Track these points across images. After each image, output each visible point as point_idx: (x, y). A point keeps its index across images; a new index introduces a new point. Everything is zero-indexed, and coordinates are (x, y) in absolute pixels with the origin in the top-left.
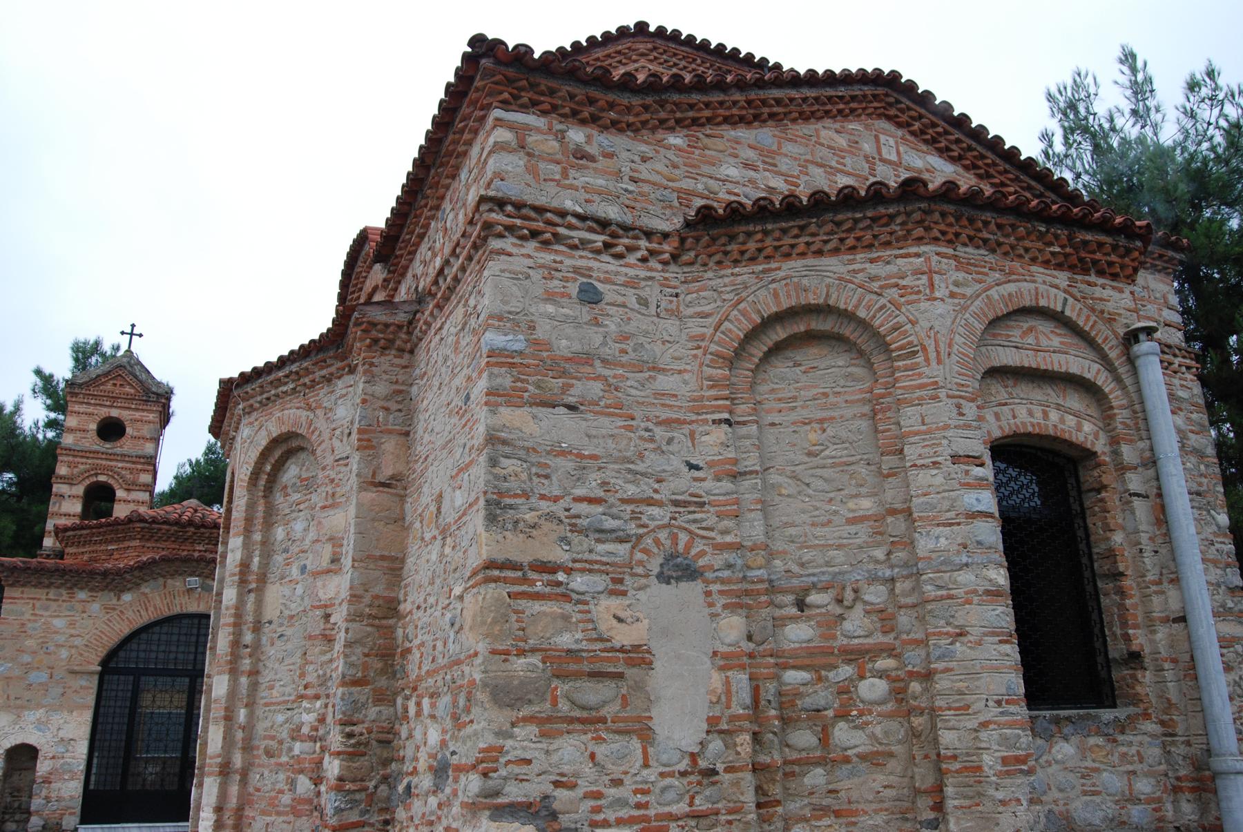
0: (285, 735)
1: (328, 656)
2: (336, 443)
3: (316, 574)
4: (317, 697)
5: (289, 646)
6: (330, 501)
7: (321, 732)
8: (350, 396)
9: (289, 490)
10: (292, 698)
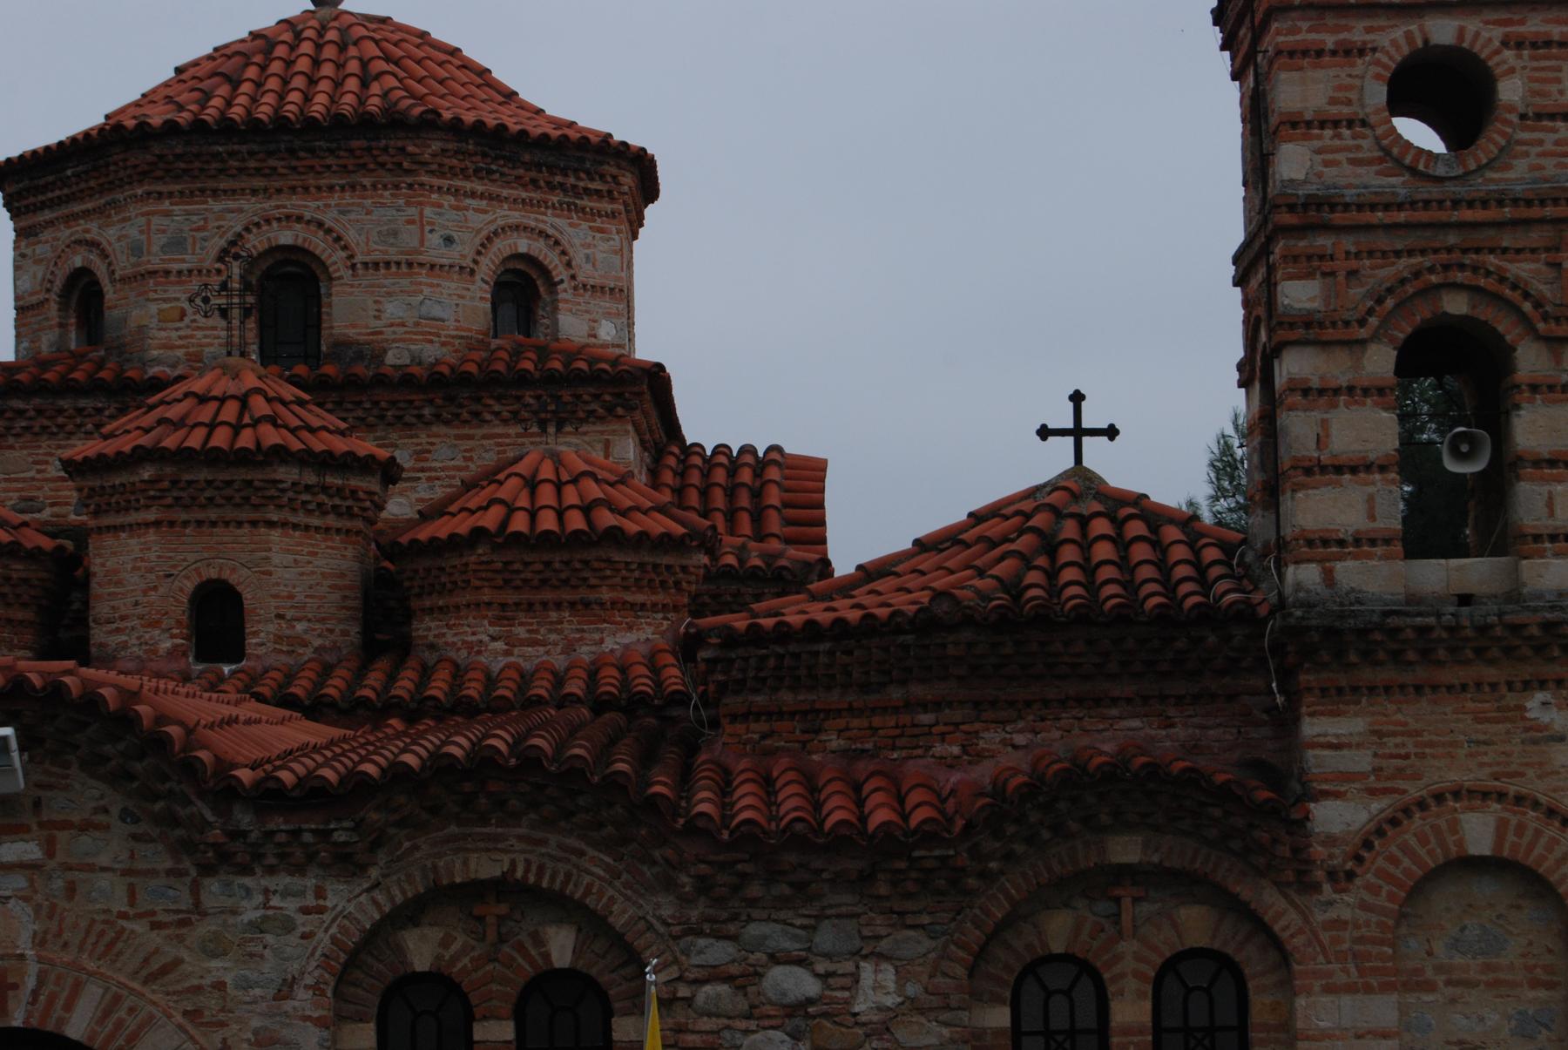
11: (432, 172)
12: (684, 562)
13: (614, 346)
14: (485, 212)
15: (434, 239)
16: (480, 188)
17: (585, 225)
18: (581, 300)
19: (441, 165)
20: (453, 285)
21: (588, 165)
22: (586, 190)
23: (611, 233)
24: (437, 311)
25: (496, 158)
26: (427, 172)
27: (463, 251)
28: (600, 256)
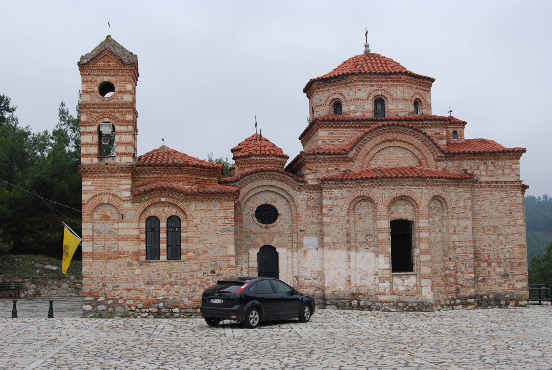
0: (440, 269)
1: (454, 253)
2: (452, 203)
3: (451, 234)
4: (453, 261)
5: (438, 249)
7: (455, 269)
15: (318, 101)
16: (326, 89)
17: (347, 89)
24: (318, 113)
27: (323, 101)
28: (351, 94)
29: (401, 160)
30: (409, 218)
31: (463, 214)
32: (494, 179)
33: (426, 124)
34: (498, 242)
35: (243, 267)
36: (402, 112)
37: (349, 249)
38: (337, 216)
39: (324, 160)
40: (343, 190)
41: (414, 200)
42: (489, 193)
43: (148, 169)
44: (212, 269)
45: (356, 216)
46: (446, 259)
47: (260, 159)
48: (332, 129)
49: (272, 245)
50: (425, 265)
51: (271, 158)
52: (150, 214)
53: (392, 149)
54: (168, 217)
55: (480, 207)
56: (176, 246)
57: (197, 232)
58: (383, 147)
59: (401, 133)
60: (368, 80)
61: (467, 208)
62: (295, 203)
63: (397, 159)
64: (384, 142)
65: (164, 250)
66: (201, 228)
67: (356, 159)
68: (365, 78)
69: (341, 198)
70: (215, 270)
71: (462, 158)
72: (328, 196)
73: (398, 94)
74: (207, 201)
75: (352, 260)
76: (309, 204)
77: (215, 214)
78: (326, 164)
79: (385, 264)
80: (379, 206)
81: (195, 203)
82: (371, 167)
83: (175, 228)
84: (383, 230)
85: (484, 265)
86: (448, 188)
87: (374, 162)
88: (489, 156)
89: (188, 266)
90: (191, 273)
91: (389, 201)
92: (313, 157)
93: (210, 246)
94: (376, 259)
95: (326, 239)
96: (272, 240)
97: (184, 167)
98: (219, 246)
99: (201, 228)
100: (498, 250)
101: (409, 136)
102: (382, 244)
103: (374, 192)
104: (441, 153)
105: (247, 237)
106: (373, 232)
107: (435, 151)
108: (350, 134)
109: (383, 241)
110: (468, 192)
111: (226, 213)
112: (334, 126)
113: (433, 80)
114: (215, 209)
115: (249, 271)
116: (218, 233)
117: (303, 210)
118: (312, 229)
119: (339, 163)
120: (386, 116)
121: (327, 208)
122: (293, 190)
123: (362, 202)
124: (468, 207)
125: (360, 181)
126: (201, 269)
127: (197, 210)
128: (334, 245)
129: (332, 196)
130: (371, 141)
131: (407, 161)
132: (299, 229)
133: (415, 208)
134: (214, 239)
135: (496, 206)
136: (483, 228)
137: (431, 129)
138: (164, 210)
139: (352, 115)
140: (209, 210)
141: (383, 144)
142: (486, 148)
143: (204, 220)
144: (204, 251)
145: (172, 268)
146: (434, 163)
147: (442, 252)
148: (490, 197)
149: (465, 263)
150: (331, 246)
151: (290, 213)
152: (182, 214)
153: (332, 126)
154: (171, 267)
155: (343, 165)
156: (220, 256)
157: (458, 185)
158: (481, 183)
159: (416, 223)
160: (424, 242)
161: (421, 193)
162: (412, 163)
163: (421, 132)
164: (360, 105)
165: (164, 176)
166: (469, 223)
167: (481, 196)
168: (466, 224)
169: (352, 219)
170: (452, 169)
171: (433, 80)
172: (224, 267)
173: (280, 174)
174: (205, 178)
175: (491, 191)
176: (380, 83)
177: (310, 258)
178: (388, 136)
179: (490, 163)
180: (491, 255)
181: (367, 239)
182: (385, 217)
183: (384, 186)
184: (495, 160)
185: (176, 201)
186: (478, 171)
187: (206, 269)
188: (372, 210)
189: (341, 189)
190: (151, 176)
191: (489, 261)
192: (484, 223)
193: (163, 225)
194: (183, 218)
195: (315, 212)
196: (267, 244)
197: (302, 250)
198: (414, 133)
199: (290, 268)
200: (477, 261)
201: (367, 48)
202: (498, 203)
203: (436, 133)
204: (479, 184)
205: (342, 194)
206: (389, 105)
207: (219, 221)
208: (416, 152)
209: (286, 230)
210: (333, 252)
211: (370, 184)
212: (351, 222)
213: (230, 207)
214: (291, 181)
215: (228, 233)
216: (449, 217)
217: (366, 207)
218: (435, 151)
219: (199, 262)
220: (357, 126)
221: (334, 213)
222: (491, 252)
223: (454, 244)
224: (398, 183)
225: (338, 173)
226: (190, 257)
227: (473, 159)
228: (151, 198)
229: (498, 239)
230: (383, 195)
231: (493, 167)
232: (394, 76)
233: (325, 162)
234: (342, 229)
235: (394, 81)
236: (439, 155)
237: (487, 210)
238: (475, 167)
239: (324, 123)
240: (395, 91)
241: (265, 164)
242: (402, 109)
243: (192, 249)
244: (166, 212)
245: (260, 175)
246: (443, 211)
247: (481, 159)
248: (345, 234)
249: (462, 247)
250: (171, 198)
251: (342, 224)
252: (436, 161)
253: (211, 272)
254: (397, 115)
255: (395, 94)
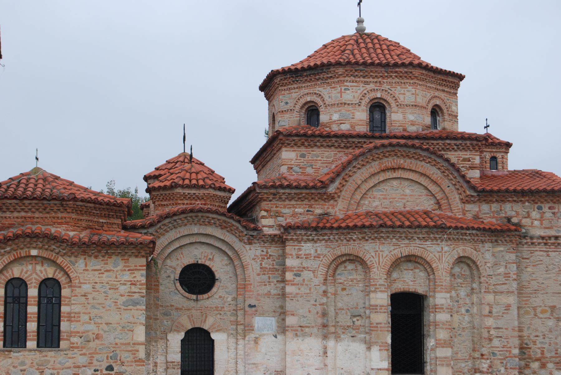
0: (466, 371)
1: (489, 346)
2: (487, 269)
4: (488, 359)
6: (487, 290)
7: (490, 370)
8: (491, 251)
9: (456, 277)
10: (467, 358)
11: (281, 86)
12: (173, 192)
13: (337, 121)
14: (297, 92)
15: (283, 104)
16: (296, 86)
17: (329, 87)
18: (327, 110)
19: (283, 83)
20: (288, 115)
21: (325, 70)
22: (328, 77)
23: (337, 87)
24: (282, 123)
25: (297, 77)
26: (281, 86)
27: (290, 105)
28: (333, 95)
29: (410, 199)
30: (421, 290)
31: (503, 286)
32: (553, 233)
33: (449, 144)
34: (556, 331)
35: (158, 361)
36: (413, 125)
37: (325, 337)
38: (307, 285)
39: (290, 196)
40: (317, 245)
41: (428, 263)
42: (545, 254)
43: (11, 204)
44: (108, 364)
45: (337, 285)
46: (477, 355)
47: (190, 192)
48: (303, 149)
49: (204, 328)
50: (443, 365)
51: (206, 192)
52: (13, 274)
53: (395, 183)
54: (41, 280)
55: (530, 275)
56: (53, 326)
57: (86, 304)
58: (382, 179)
59: (410, 158)
60: (362, 74)
61: (509, 277)
62: (242, 263)
63: (403, 199)
64: (383, 171)
65: (33, 332)
66: (94, 299)
67: (339, 197)
68: (356, 71)
69: (315, 257)
70: (114, 365)
71: (503, 199)
72: (294, 253)
73: (407, 98)
74: (103, 256)
75: (328, 354)
76: (263, 265)
77: (116, 278)
78: (293, 202)
79: (382, 361)
80: (374, 270)
81: (85, 259)
82: (363, 210)
83: (52, 298)
84: (378, 308)
85: (535, 365)
86: (481, 245)
87: (367, 202)
88: (546, 196)
89: (70, 358)
90: (75, 369)
91: (389, 263)
92: (272, 191)
93: (106, 328)
94: (368, 353)
95: (290, 321)
96: (205, 321)
97: (68, 203)
98: (120, 328)
99: (94, 299)
100: (556, 344)
101: (423, 163)
102: (377, 331)
103: (367, 248)
104: (472, 191)
105: (165, 314)
106: (362, 310)
107: (462, 187)
108: (331, 157)
109: (379, 326)
110: (512, 253)
111: (134, 275)
112: (306, 143)
113: (461, 77)
114: (115, 269)
115: (168, 368)
116: (120, 306)
117: (255, 275)
118: (269, 304)
119: (312, 202)
120: (388, 131)
121: (293, 271)
122: (239, 243)
123: (347, 263)
124: (511, 275)
125: (345, 231)
126: (92, 363)
127: (87, 270)
128: (302, 330)
129: (300, 253)
130: (364, 168)
131: (418, 201)
132: (247, 303)
133: (429, 276)
134: (114, 317)
135: (554, 275)
136: (535, 309)
137: (456, 153)
138: (34, 269)
139: (335, 128)
140: (107, 271)
141: (382, 174)
142: (541, 185)
143: (98, 286)
144: (98, 334)
145: (46, 360)
146: (460, 206)
147: (470, 345)
148: (546, 260)
149: (505, 362)
150: (297, 330)
151: (234, 278)
152: (63, 275)
153: (303, 144)
154: (43, 359)
155: (319, 204)
156: (122, 344)
157: (496, 241)
158: (532, 238)
159: (431, 299)
160: (443, 328)
161: (438, 252)
162: (427, 204)
163: (441, 157)
164: (348, 113)
165: (37, 215)
166: (512, 300)
167: (532, 259)
168: (509, 302)
169: (331, 290)
170: (488, 215)
171: (461, 77)
172: (128, 362)
173: (219, 217)
174: (101, 221)
175: (548, 251)
176: (380, 79)
177: (263, 350)
178: (389, 162)
179: (547, 208)
180: (545, 350)
181: (353, 322)
182: (383, 288)
183: (382, 239)
184: (554, 203)
185: (54, 255)
186: (528, 219)
187: (99, 363)
188: (362, 277)
189: (316, 242)
190: (16, 214)
191: (543, 360)
192: (536, 301)
193: (33, 292)
194: (64, 282)
195: (274, 277)
196: (197, 326)
197: (252, 336)
198: (430, 158)
199: (232, 365)
200: (525, 359)
201: (360, 25)
202: (558, 269)
203: (464, 160)
204: (529, 240)
205: (316, 251)
206: (392, 114)
207: (123, 289)
208: (433, 188)
209: (227, 304)
210: (300, 340)
211: (360, 236)
212: (329, 295)
213: (140, 266)
214: (237, 228)
215: (135, 308)
216: (483, 290)
217: (354, 272)
218: (462, 187)
219: (88, 353)
220: (342, 145)
221: (304, 280)
222: (546, 346)
223: (489, 332)
224: (403, 235)
225: (311, 217)
226: (73, 344)
227: (521, 201)
228: (15, 250)
229: (557, 326)
230: (381, 253)
231: (551, 215)
232: (401, 70)
233: (290, 200)
234: (315, 305)
235: (401, 77)
236: (468, 193)
237: (541, 280)
238: (524, 213)
239: (291, 139)
240: (402, 92)
241: (196, 200)
242: (412, 121)
243: (78, 332)
244: (39, 273)
245: (189, 218)
246: (473, 281)
247: (533, 201)
248: (320, 312)
249: (501, 337)
250: (46, 249)
251: (314, 297)
252: (464, 203)
253: (107, 369)
254: (405, 130)
255: (401, 97)
